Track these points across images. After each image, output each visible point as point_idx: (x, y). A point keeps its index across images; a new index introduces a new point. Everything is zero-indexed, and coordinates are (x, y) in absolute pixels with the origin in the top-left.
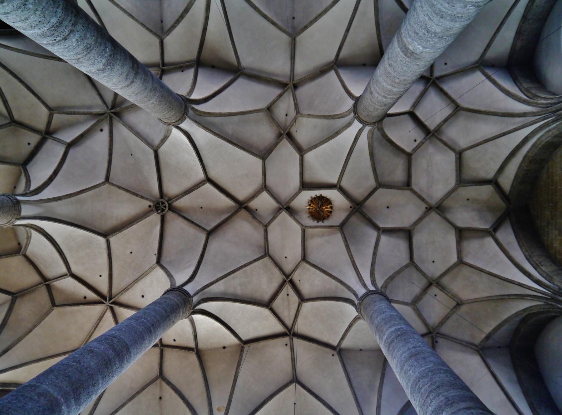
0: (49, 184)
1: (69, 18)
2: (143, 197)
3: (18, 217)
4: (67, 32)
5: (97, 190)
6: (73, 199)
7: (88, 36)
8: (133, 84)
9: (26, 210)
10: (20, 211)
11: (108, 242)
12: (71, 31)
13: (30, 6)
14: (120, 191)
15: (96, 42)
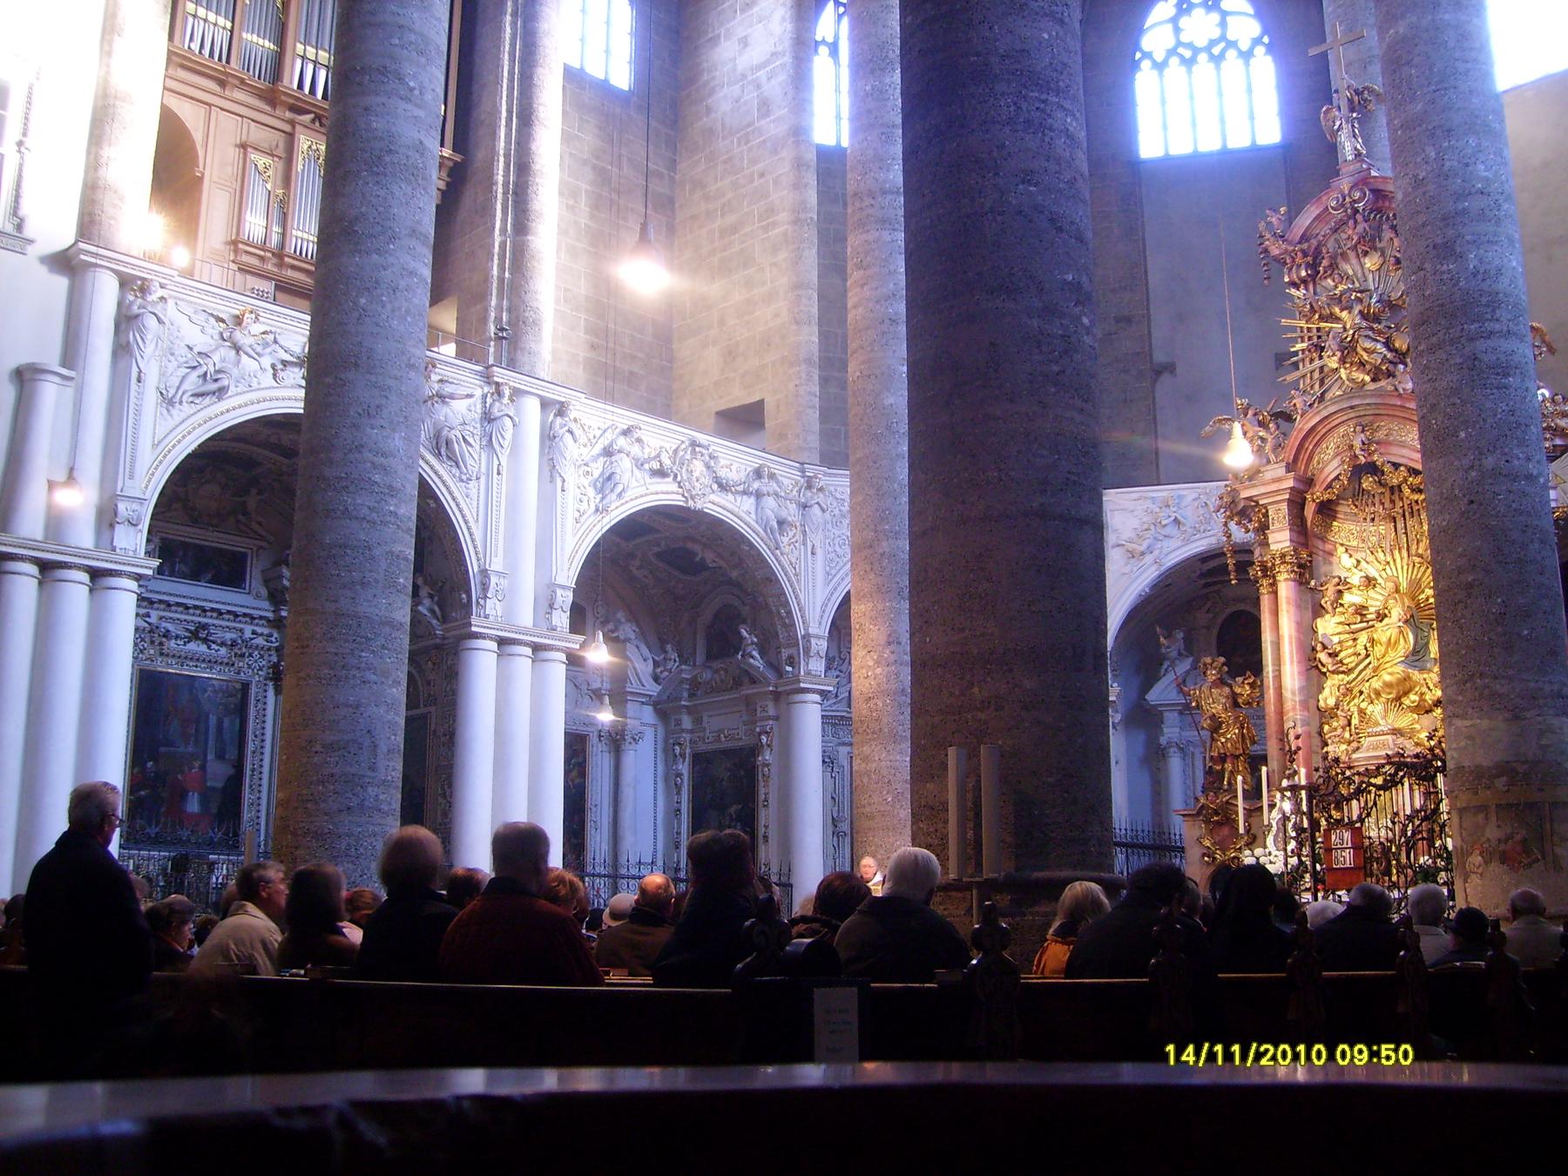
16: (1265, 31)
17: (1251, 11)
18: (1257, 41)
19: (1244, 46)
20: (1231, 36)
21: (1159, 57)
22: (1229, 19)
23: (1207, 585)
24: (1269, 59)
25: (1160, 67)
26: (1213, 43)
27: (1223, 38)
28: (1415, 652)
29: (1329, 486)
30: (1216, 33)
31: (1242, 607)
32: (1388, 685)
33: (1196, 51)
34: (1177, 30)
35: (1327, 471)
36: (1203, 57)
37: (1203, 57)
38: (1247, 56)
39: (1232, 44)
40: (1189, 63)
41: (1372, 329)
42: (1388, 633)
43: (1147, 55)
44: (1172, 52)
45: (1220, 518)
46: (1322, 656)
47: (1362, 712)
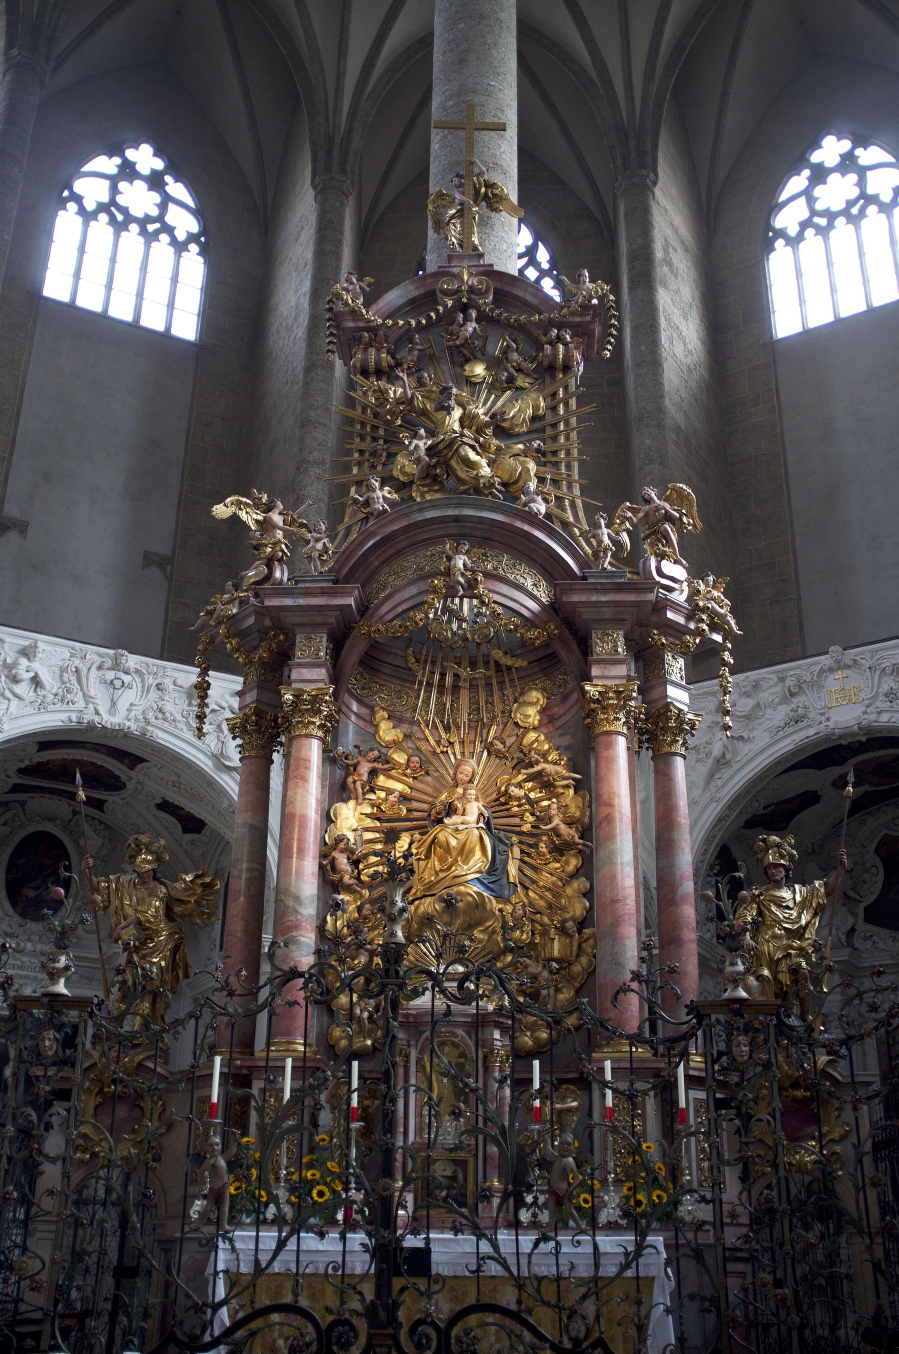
16: (204, 231)
17: (191, 203)
18: (192, 238)
19: (181, 236)
20: (169, 219)
21: (90, 206)
22: (171, 206)
23: (16, 789)
24: (201, 260)
25: (87, 216)
26: (148, 219)
27: (160, 218)
28: (492, 870)
30: (154, 212)
31: (48, 827)
33: (129, 219)
34: (114, 190)
35: (397, 599)
36: (134, 228)
37: (134, 228)
38: (180, 247)
39: (169, 230)
40: (119, 227)
41: (477, 441)
42: (461, 837)
43: (77, 199)
44: (102, 208)
46: (342, 861)
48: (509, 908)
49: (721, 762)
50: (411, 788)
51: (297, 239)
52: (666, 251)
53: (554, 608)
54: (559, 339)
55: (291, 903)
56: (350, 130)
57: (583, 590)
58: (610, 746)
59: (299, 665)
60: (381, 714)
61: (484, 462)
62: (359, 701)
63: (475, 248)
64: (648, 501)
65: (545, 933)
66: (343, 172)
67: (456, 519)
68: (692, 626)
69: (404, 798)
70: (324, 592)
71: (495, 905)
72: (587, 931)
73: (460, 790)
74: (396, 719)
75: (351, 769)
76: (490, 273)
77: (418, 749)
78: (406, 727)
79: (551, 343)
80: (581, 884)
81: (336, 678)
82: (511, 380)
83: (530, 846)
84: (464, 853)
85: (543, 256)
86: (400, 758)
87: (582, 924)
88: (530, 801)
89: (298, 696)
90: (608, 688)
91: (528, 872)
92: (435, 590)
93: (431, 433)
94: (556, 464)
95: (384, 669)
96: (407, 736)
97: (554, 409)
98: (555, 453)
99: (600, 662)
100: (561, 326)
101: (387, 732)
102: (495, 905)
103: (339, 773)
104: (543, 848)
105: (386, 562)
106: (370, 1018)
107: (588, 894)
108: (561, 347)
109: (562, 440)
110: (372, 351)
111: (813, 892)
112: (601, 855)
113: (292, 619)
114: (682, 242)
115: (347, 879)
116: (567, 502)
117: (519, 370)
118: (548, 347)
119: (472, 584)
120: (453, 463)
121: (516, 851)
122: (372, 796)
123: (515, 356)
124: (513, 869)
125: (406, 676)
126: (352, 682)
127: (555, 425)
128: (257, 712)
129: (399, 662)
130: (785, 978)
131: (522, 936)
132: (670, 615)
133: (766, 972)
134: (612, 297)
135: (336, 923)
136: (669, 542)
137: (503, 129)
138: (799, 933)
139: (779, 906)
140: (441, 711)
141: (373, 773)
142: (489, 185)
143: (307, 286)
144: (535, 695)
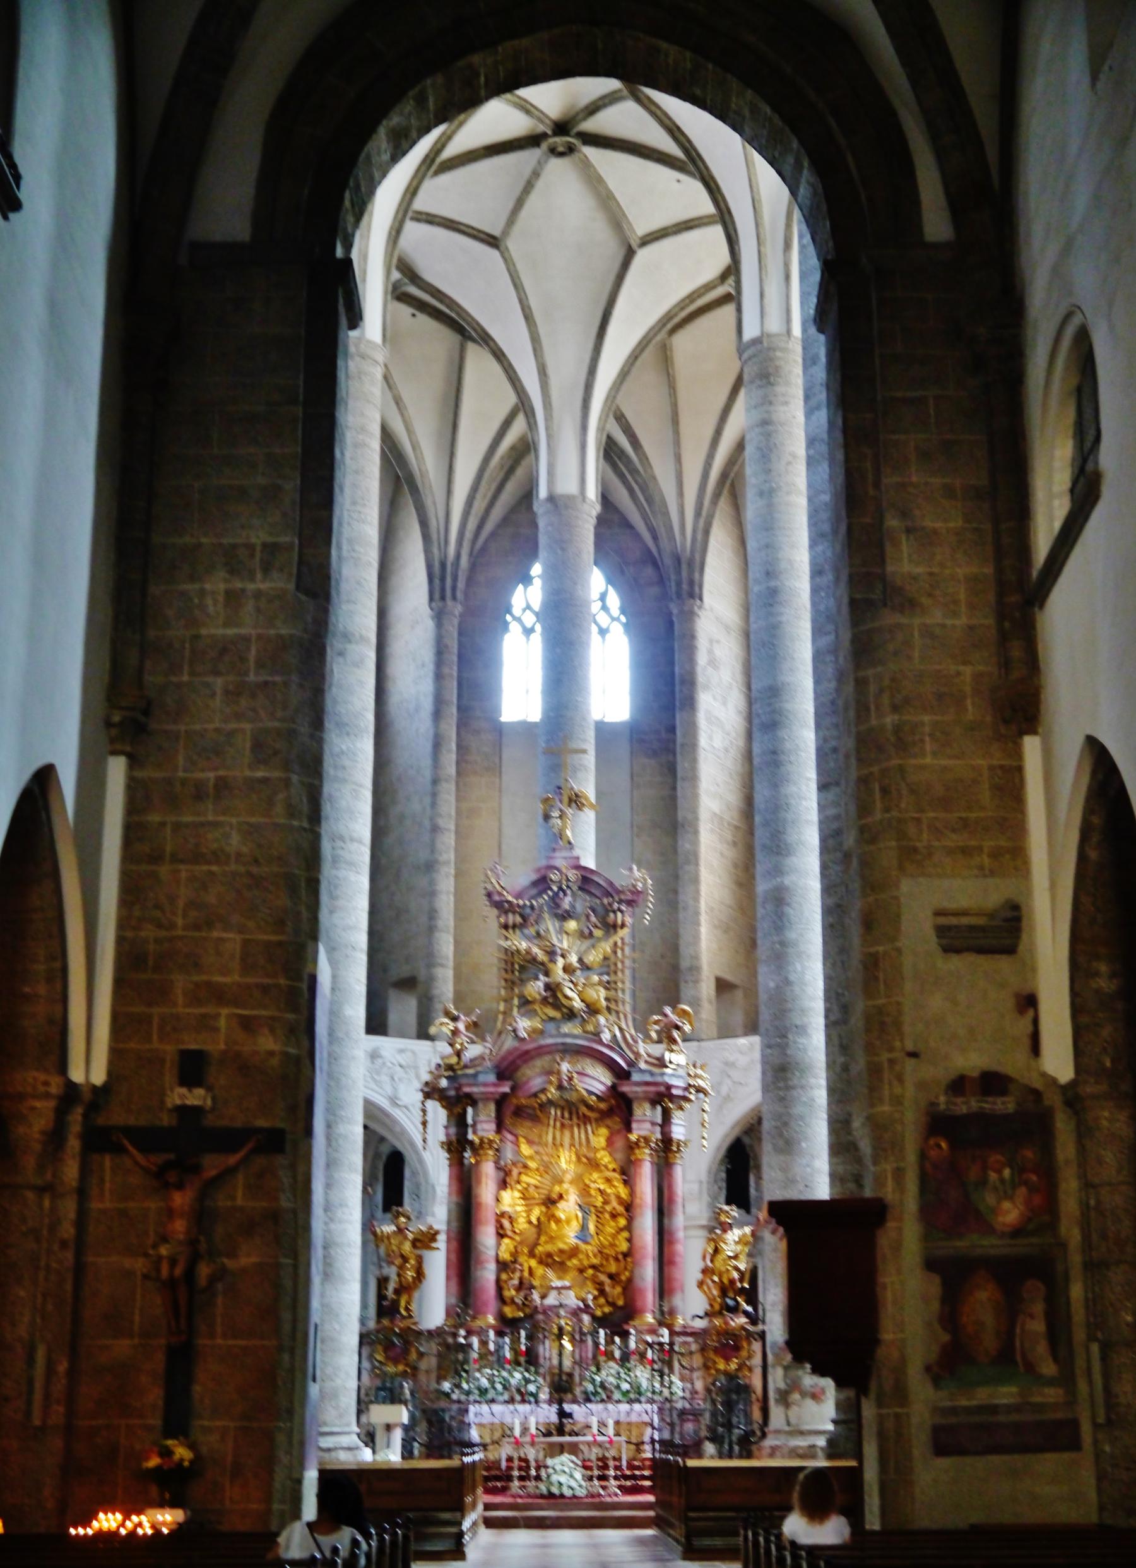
0: (510, 365)
1: (340, 852)
2: (536, 174)
3: (580, 498)
4: (356, 844)
5: (520, 267)
6: (542, 330)
7: (343, 803)
8: (364, 632)
9: (567, 485)
10: (570, 498)
11: (648, 240)
12: (352, 840)
13: (354, 919)
14: (524, 213)
15: (345, 781)
29: (535, 1095)
32: (561, 1251)
41: (572, 981)
45: (420, 1096)
46: (506, 1223)
47: (530, 1269)
48: (589, 1247)
49: (728, 1098)
50: (539, 1181)
51: (413, 627)
52: (710, 652)
53: (613, 1088)
54: (620, 910)
55: (482, 1248)
56: (458, 556)
57: (628, 1085)
58: (640, 1166)
59: (481, 1122)
60: (522, 1140)
61: (577, 998)
62: (511, 1133)
63: (570, 843)
64: (666, 1015)
65: (607, 1260)
66: (454, 598)
67: (563, 1044)
68: (687, 1094)
69: (536, 1187)
70: (494, 1085)
71: (583, 1246)
72: (629, 1259)
73: (566, 1186)
74: (530, 1142)
75: (507, 1173)
76: (579, 867)
77: (543, 1160)
78: (536, 1148)
79: (614, 912)
80: (625, 1234)
81: (500, 1127)
82: (591, 934)
83: (600, 1212)
84: (568, 1222)
85: (614, 600)
86: (532, 1164)
87: (626, 1255)
88: (600, 1190)
89: (481, 1140)
90: (640, 1136)
91: (600, 1226)
92: (551, 1082)
93: (547, 974)
94: (616, 990)
95: (525, 1115)
96: (536, 1153)
97: (615, 953)
98: (615, 983)
99: (638, 1121)
100: (620, 902)
101: (526, 1150)
102: (583, 1246)
103: (502, 1174)
104: (607, 1216)
105: (526, 1062)
106: (524, 1304)
107: (629, 1240)
108: (619, 914)
109: (620, 974)
110: (510, 916)
111: (744, 1235)
112: (637, 1223)
113: (475, 1096)
114: (727, 628)
115: (509, 1233)
116: (622, 1016)
117: (596, 927)
118: (612, 915)
119: (571, 1079)
120: (559, 995)
121: (594, 1217)
122: (519, 1187)
123: (593, 919)
124: (592, 1227)
125: (535, 1119)
126: (508, 1121)
127: (616, 964)
128: (458, 1141)
129: (530, 1111)
130: (725, 1281)
131: (595, 1261)
132: (675, 1092)
133: (716, 1279)
134: (650, 882)
135: (505, 1256)
136: (674, 1041)
137: (584, 751)
138: (736, 1257)
139: (726, 1243)
140: (554, 1138)
141: (520, 1173)
142: (577, 795)
143: (426, 687)
144: (604, 1132)
